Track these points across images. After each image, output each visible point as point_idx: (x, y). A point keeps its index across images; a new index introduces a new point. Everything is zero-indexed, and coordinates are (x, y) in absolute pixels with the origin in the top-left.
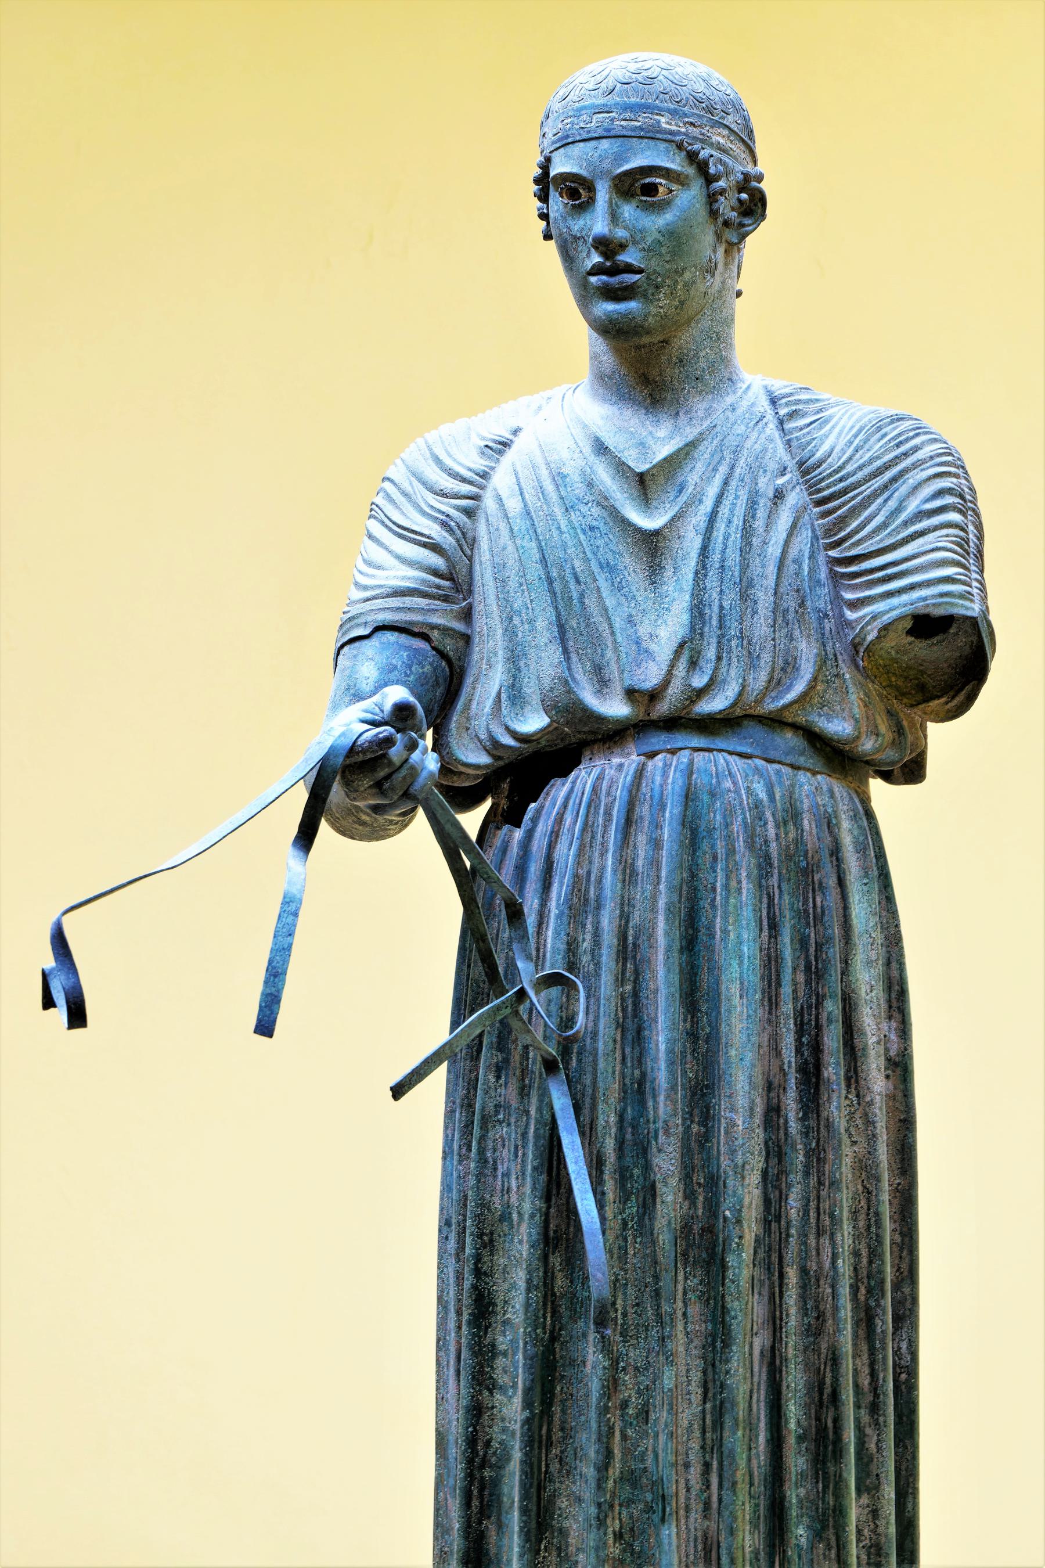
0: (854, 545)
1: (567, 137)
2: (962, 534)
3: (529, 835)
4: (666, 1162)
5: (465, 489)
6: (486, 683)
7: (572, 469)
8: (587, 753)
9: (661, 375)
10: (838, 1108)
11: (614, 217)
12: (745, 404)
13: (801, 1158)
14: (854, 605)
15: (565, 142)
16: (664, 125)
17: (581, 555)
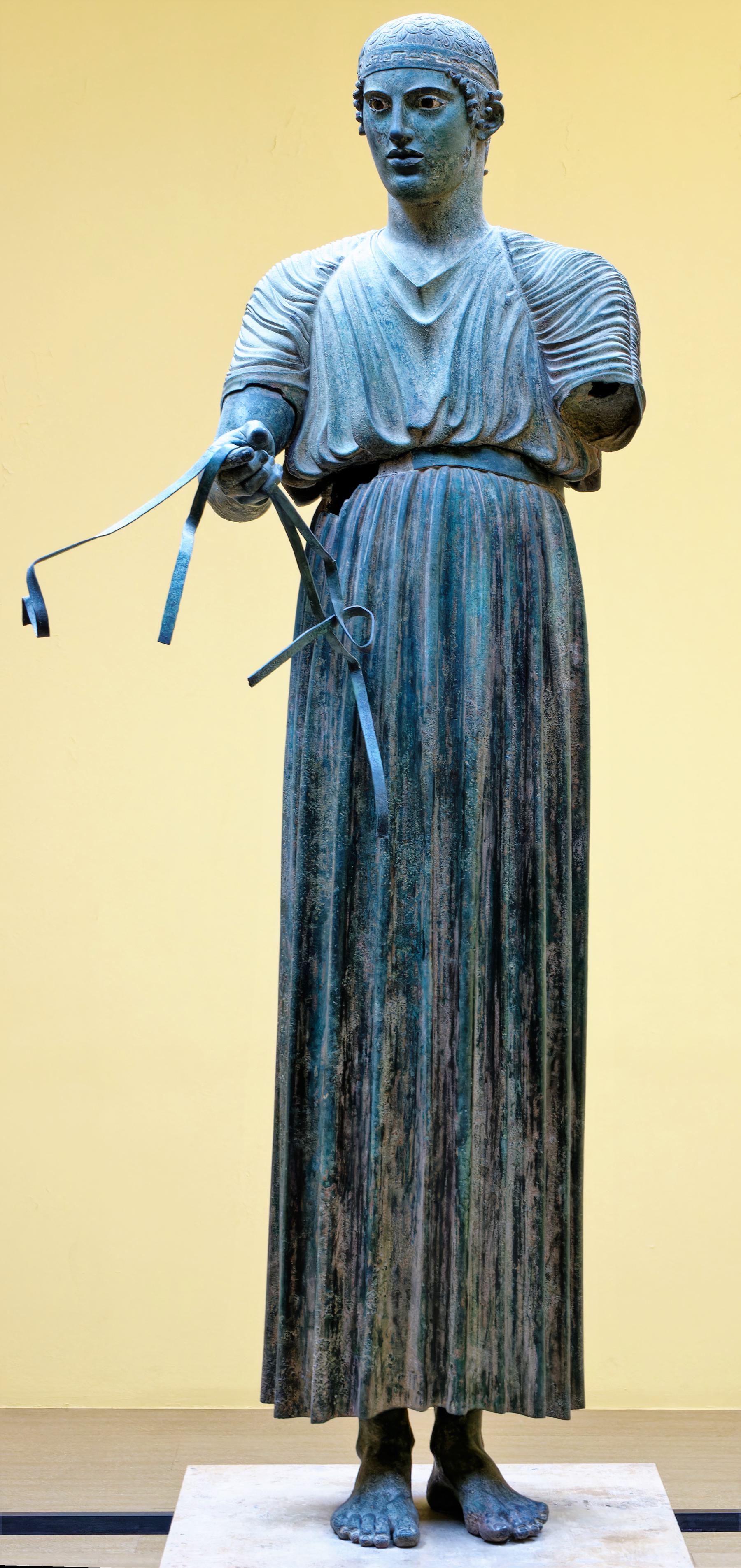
0: (556, 336)
1: (375, 67)
2: (625, 330)
3: (345, 519)
4: (429, 731)
5: (307, 296)
6: (318, 421)
7: (375, 284)
8: (382, 468)
9: (434, 224)
10: (539, 697)
11: (404, 121)
12: (488, 244)
13: (515, 728)
14: (555, 375)
15: (374, 71)
17: (380, 340)
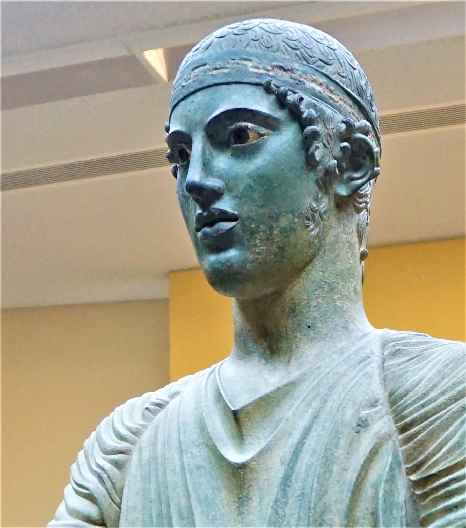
11: (207, 167)
16: (251, 70)
